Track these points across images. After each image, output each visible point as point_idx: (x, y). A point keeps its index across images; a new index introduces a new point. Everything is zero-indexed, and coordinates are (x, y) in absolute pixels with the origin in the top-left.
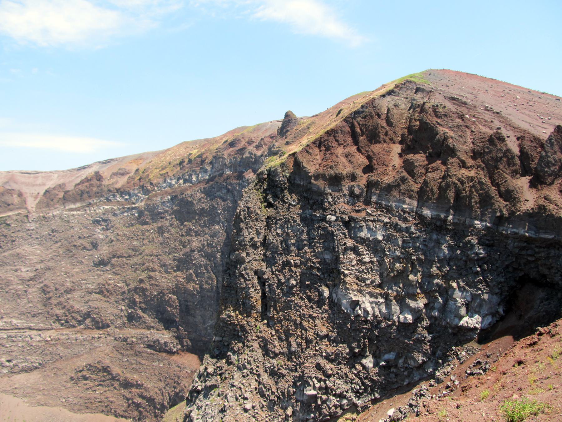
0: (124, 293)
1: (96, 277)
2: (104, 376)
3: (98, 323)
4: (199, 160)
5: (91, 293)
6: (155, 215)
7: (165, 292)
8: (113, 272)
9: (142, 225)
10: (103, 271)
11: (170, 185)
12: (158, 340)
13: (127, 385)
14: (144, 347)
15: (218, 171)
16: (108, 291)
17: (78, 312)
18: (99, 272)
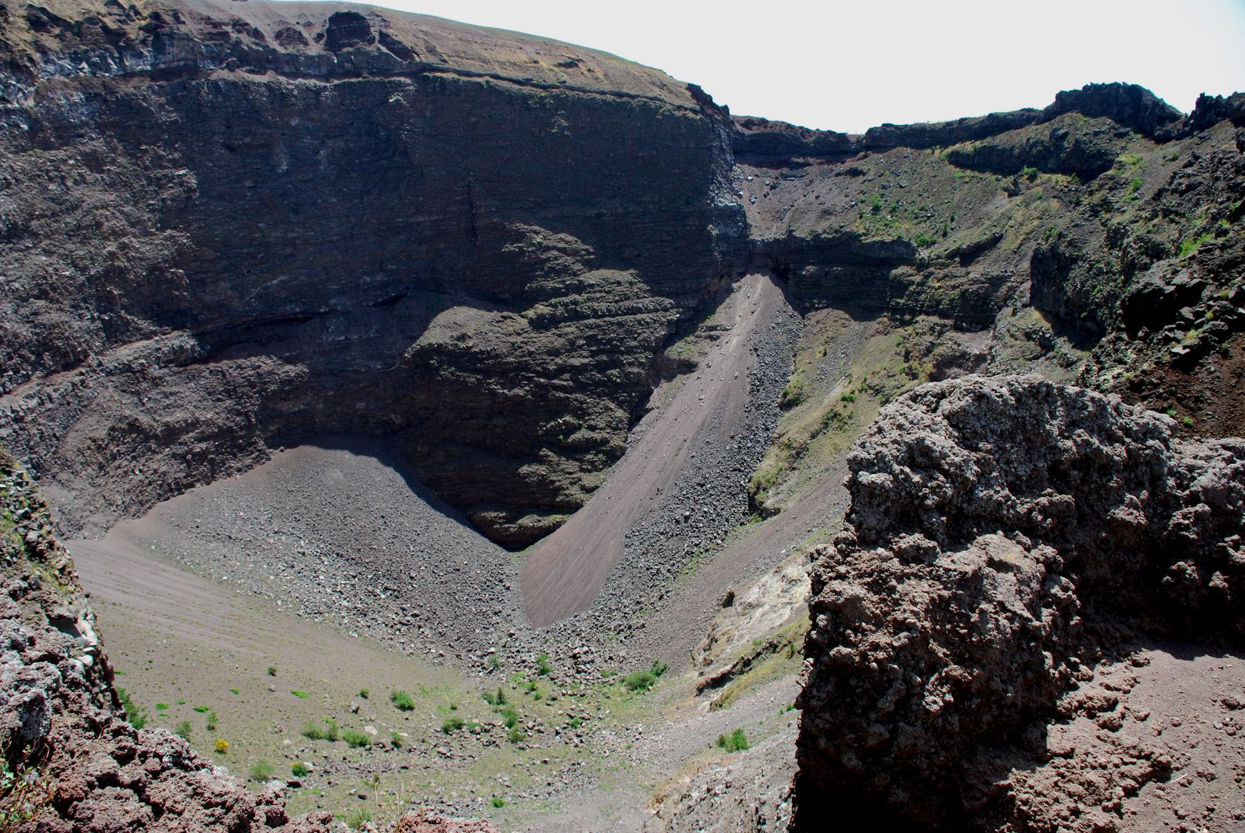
0: (80, 288)
1: (16, 265)
2: (134, 440)
3: (66, 355)
4: (98, 29)
5: (26, 300)
6: (66, 133)
7: (162, 264)
8: (44, 250)
9: (44, 150)
10: (21, 250)
11: (62, 70)
12: (181, 347)
13: (171, 435)
14: (160, 368)
15: (178, 61)
16: (54, 289)
17: (27, 344)
18: (16, 255)
